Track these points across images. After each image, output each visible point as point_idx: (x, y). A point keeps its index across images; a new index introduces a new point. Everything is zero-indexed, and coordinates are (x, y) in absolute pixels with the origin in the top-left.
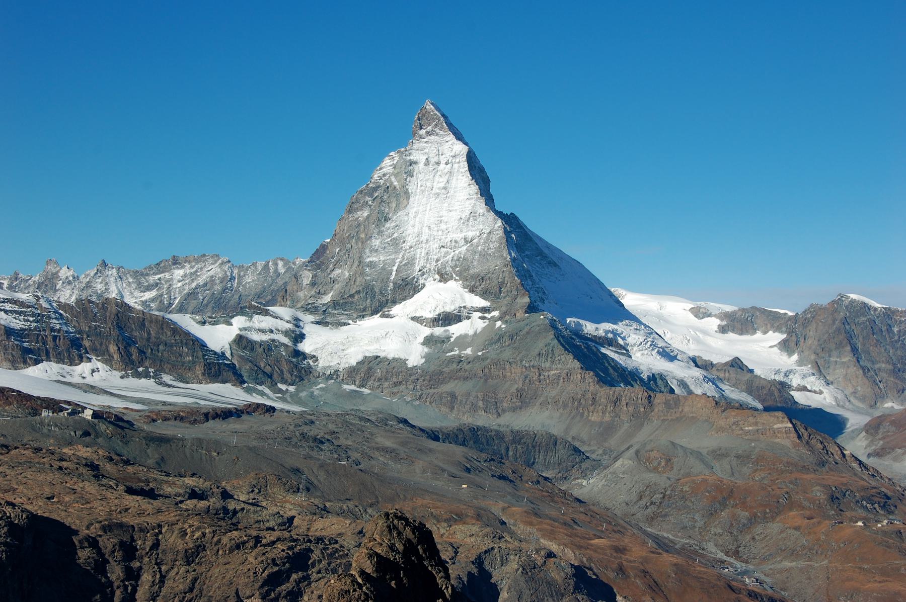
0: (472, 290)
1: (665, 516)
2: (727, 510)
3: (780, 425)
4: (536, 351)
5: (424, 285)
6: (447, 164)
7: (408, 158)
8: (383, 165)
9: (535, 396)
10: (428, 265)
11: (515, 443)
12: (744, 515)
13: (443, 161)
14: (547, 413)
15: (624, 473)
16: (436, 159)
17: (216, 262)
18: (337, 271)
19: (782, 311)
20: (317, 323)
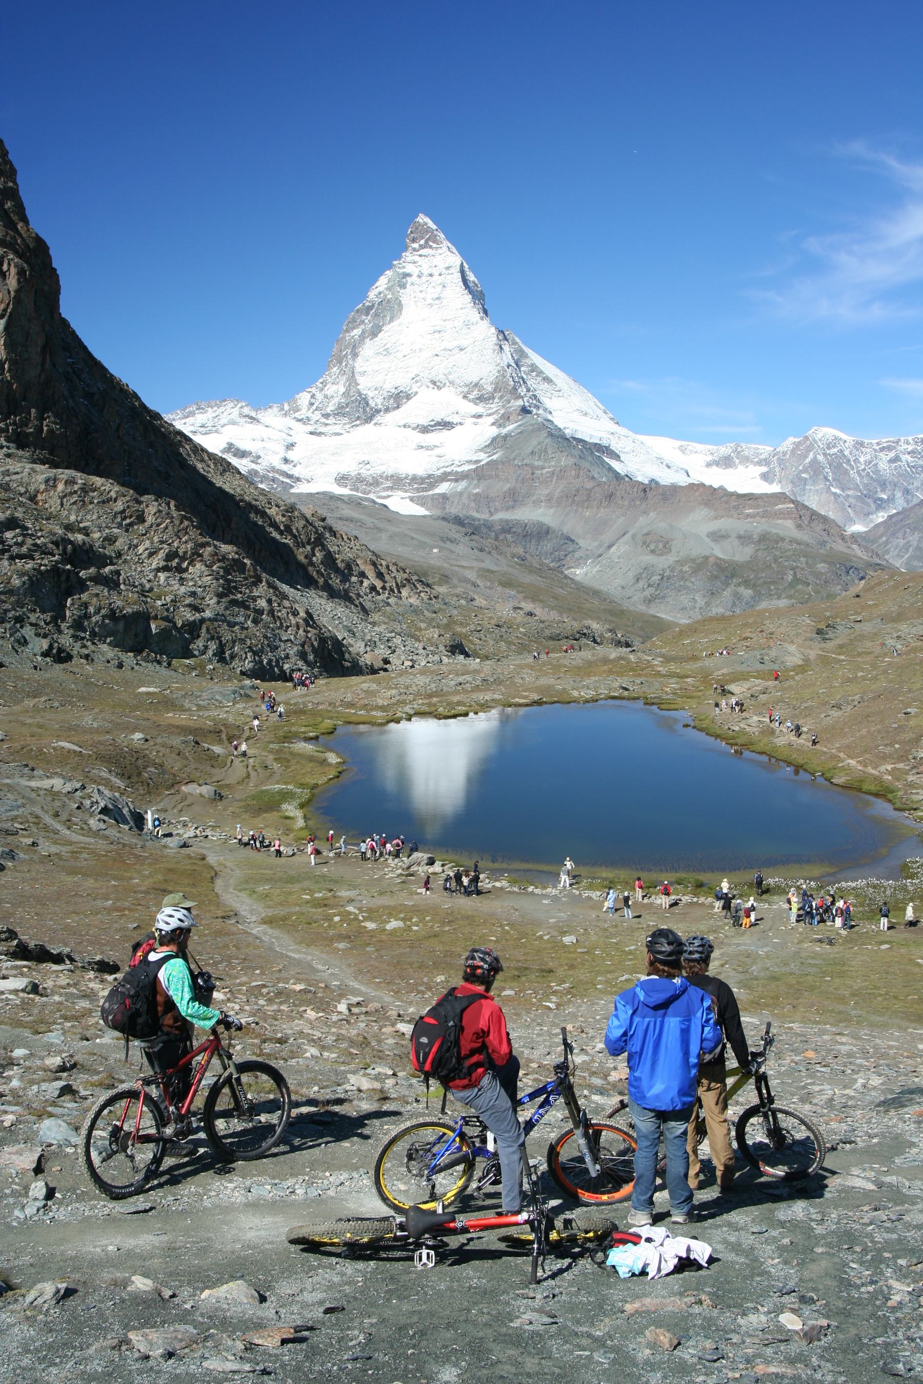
0: (465, 397)
1: (663, 597)
2: (729, 589)
4: (530, 449)
6: (440, 275)
7: (401, 271)
9: (528, 495)
11: (505, 532)
12: (747, 593)
13: (436, 273)
14: (541, 511)
15: (619, 557)
16: (430, 271)
17: (236, 405)
18: (335, 388)
20: (311, 433)
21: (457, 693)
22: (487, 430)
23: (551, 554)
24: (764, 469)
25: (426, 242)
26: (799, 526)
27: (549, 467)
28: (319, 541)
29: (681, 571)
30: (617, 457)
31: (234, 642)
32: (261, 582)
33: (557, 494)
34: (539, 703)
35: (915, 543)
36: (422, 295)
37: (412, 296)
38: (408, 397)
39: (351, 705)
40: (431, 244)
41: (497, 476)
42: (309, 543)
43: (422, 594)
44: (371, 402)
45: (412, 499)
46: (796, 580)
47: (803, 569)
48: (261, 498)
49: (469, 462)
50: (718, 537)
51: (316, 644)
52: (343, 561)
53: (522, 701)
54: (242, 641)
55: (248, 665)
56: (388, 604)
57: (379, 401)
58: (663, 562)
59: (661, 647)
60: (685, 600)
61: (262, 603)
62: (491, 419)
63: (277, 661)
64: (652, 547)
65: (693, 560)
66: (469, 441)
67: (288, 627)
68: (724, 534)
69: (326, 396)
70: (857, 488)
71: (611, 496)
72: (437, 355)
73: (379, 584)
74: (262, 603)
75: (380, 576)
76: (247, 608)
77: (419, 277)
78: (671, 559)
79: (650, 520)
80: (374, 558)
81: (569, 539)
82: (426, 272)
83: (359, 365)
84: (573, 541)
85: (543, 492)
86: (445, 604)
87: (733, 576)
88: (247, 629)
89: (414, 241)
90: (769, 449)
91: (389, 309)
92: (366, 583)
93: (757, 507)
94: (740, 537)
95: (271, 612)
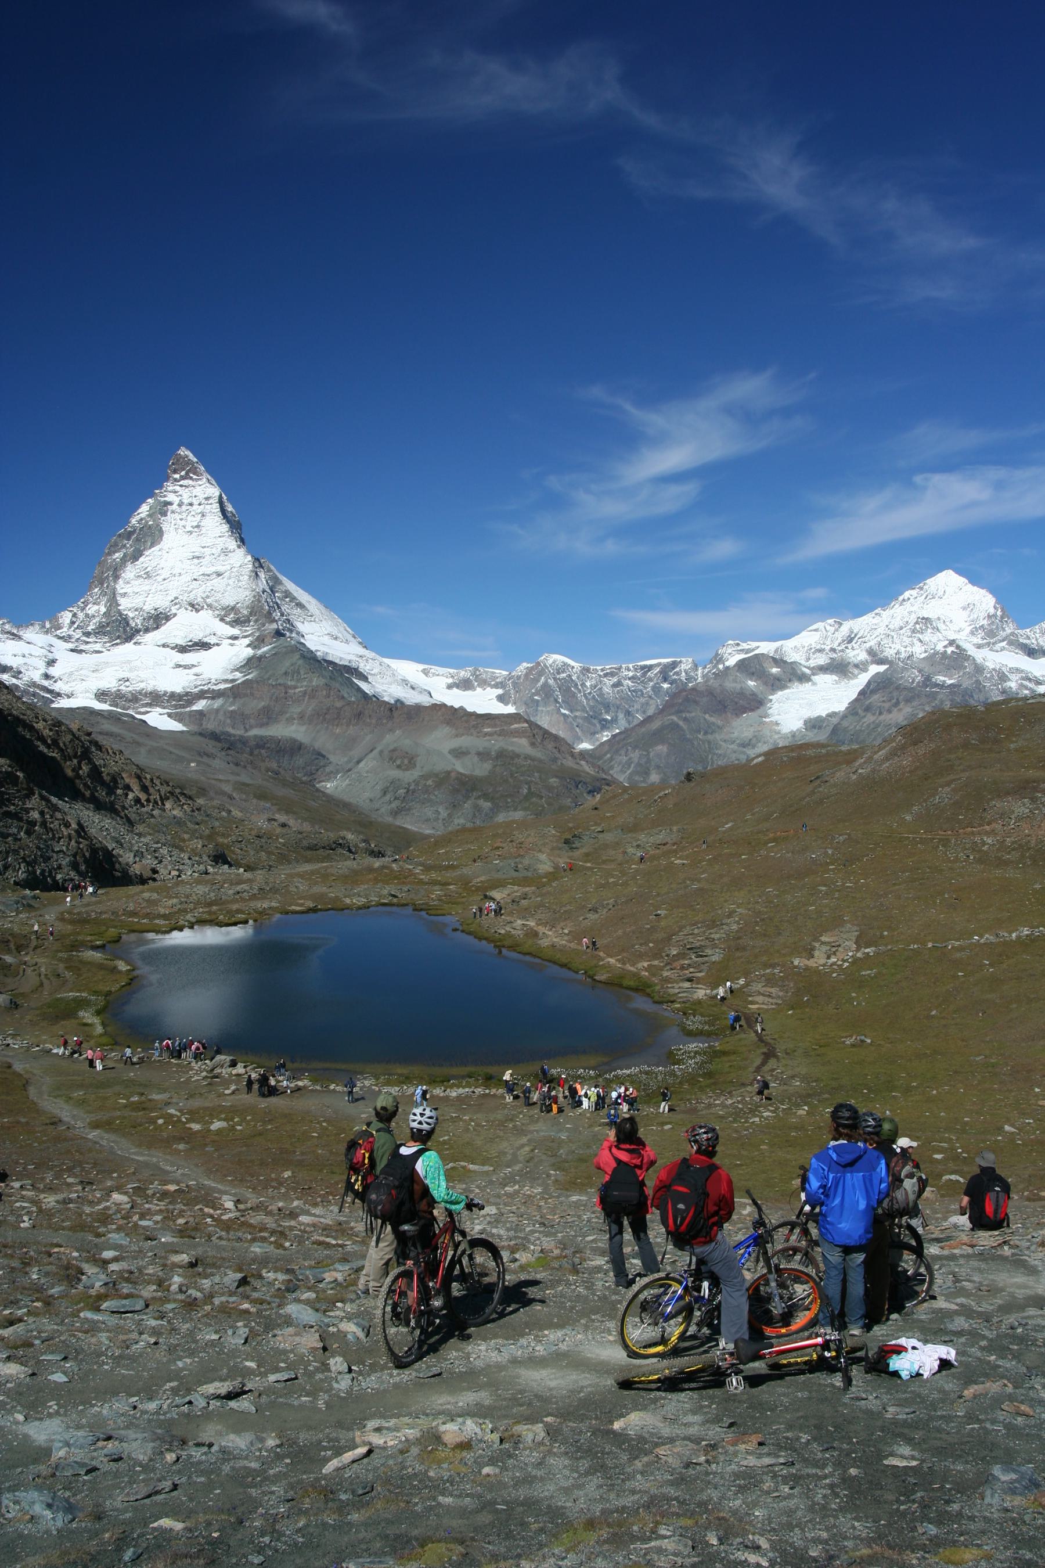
0: (222, 620)
1: (409, 810)
2: (469, 802)
4: (283, 670)
5: (175, 615)
6: (200, 504)
8: (140, 511)
9: (282, 713)
12: (486, 805)
13: (195, 502)
14: (293, 728)
15: (367, 772)
16: (190, 500)
18: (96, 607)
20: (72, 650)
21: (235, 901)
22: (242, 651)
23: (303, 768)
24: (500, 691)
25: (187, 473)
26: (533, 744)
28: (86, 755)
29: (425, 785)
30: (365, 678)
31: (8, 853)
32: (34, 794)
33: (309, 711)
34: (314, 910)
35: (636, 760)
36: (183, 523)
38: (168, 618)
39: (133, 914)
41: (252, 694)
42: (75, 756)
43: (185, 807)
44: (131, 622)
45: (170, 715)
46: (530, 794)
47: (536, 783)
48: (29, 712)
49: (226, 681)
50: (459, 753)
51: (87, 854)
52: (108, 774)
53: (298, 908)
54: (16, 852)
55: (21, 875)
56: (153, 816)
57: (139, 622)
58: (409, 776)
59: (418, 857)
60: (429, 812)
61: (35, 815)
62: (247, 641)
63: (50, 872)
64: (398, 762)
65: (437, 775)
66: (226, 659)
67: (60, 838)
68: (464, 750)
69: (87, 616)
70: (584, 710)
71: (360, 714)
73: (143, 797)
74: (35, 815)
75: (144, 789)
76: (20, 819)
77: (180, 505)
78: (414, 774)
79: (394, 738)
80: (139, 772)
81: (320, 754)
82: (186, 501)
83: (121, 587)
84: (324, 756)
85: (296, 710)
86: (208, 816)
87: (474, 789)
88: (20, 840)
89: (175, 472)
91: (151, 535)
92: (131, 796)
93: (495, 726)
94: (479, 754)
95: (44, 824)
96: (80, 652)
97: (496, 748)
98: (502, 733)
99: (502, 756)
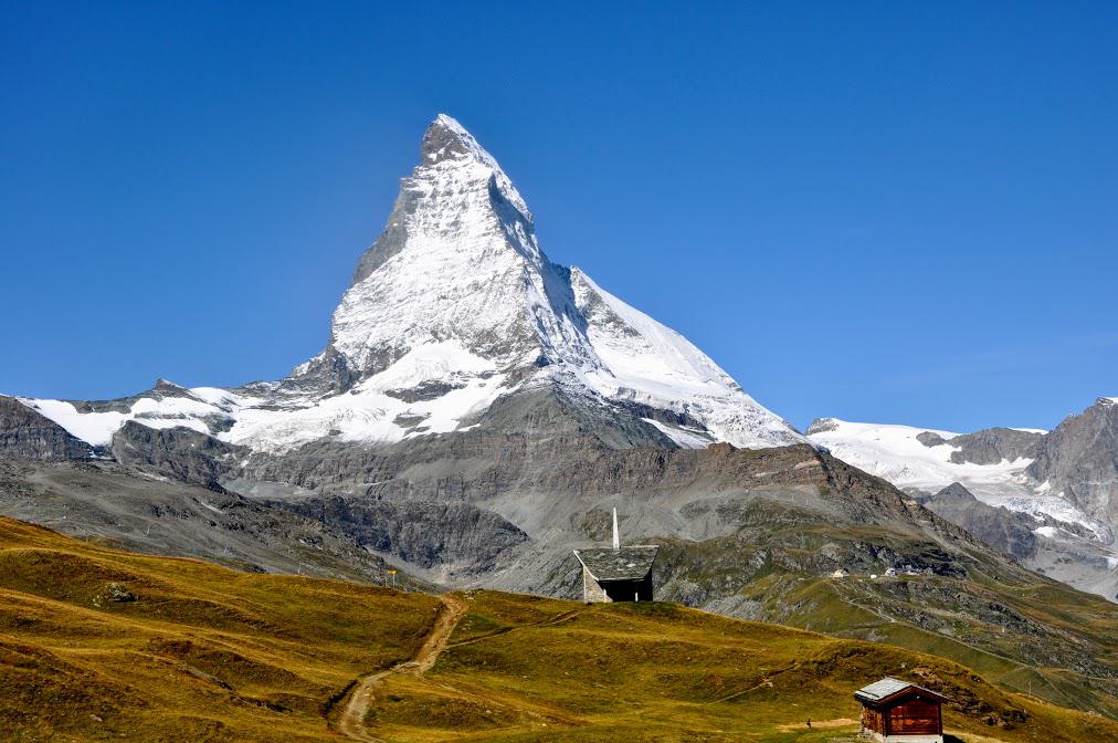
0: (473, 351)
3: (801, 465)
6: (461, 192)
9: (517, 475)
10: (419, 324)
13: (455, 189)
19: (1033, 431)
20: (262, 407)
23: (478, 549)
25: (447, 151)
26: (824, 493)
27: (548, 435)
36: (434, 221)
37: (421, 223)
38: (399, 355)
40: (453, 153)
62: (502, 378)
71: (616, 470)
72: (444, 298)
77: (433, 196)
82: (441, 189)
90: (1044, 432)
93: (769, 468)
94: (721, 510)
96: (276, 408)
97: (750, 499)
98: (779, 478)
99: (756, 513)
